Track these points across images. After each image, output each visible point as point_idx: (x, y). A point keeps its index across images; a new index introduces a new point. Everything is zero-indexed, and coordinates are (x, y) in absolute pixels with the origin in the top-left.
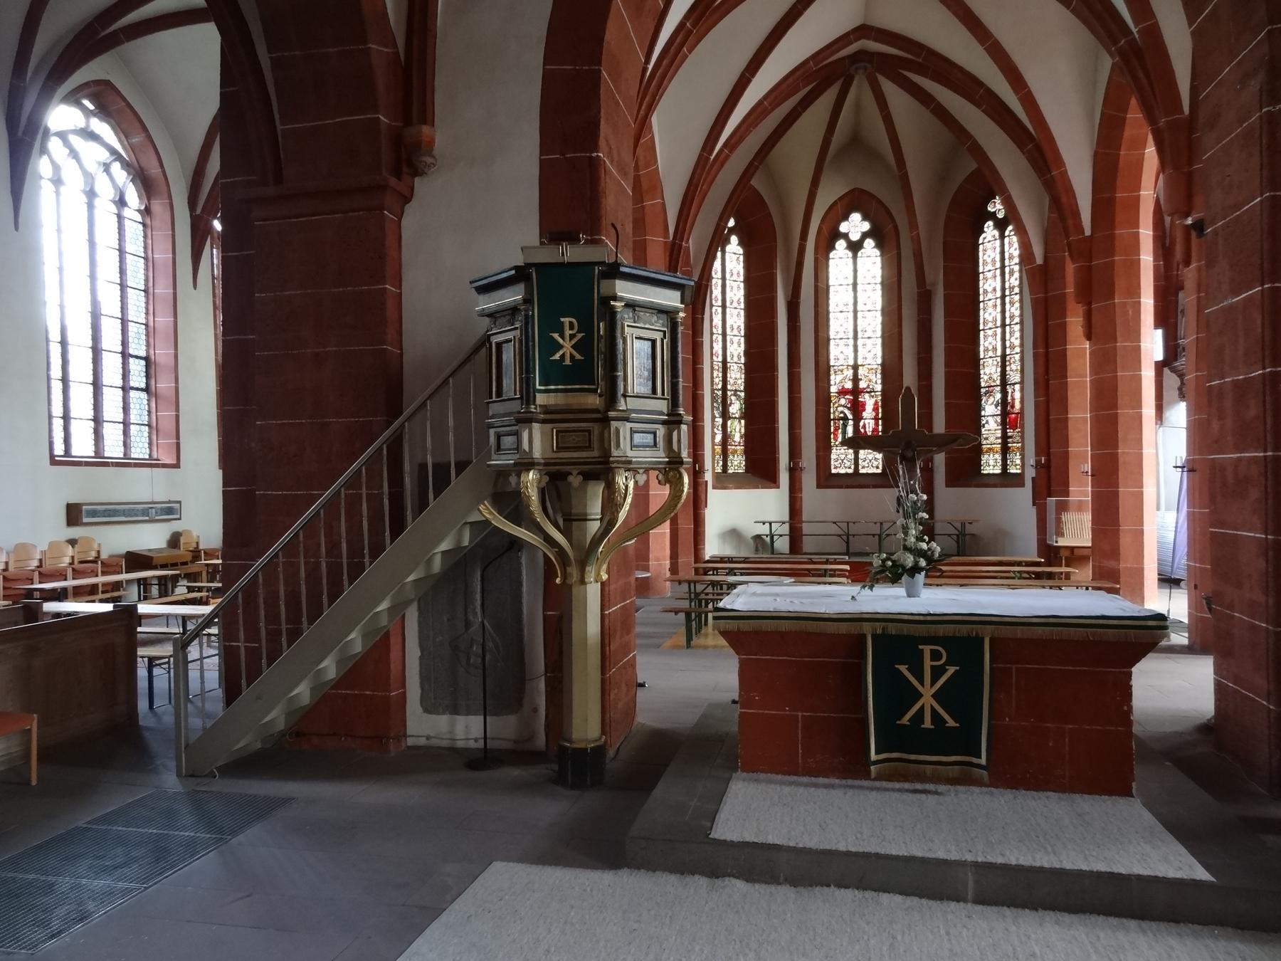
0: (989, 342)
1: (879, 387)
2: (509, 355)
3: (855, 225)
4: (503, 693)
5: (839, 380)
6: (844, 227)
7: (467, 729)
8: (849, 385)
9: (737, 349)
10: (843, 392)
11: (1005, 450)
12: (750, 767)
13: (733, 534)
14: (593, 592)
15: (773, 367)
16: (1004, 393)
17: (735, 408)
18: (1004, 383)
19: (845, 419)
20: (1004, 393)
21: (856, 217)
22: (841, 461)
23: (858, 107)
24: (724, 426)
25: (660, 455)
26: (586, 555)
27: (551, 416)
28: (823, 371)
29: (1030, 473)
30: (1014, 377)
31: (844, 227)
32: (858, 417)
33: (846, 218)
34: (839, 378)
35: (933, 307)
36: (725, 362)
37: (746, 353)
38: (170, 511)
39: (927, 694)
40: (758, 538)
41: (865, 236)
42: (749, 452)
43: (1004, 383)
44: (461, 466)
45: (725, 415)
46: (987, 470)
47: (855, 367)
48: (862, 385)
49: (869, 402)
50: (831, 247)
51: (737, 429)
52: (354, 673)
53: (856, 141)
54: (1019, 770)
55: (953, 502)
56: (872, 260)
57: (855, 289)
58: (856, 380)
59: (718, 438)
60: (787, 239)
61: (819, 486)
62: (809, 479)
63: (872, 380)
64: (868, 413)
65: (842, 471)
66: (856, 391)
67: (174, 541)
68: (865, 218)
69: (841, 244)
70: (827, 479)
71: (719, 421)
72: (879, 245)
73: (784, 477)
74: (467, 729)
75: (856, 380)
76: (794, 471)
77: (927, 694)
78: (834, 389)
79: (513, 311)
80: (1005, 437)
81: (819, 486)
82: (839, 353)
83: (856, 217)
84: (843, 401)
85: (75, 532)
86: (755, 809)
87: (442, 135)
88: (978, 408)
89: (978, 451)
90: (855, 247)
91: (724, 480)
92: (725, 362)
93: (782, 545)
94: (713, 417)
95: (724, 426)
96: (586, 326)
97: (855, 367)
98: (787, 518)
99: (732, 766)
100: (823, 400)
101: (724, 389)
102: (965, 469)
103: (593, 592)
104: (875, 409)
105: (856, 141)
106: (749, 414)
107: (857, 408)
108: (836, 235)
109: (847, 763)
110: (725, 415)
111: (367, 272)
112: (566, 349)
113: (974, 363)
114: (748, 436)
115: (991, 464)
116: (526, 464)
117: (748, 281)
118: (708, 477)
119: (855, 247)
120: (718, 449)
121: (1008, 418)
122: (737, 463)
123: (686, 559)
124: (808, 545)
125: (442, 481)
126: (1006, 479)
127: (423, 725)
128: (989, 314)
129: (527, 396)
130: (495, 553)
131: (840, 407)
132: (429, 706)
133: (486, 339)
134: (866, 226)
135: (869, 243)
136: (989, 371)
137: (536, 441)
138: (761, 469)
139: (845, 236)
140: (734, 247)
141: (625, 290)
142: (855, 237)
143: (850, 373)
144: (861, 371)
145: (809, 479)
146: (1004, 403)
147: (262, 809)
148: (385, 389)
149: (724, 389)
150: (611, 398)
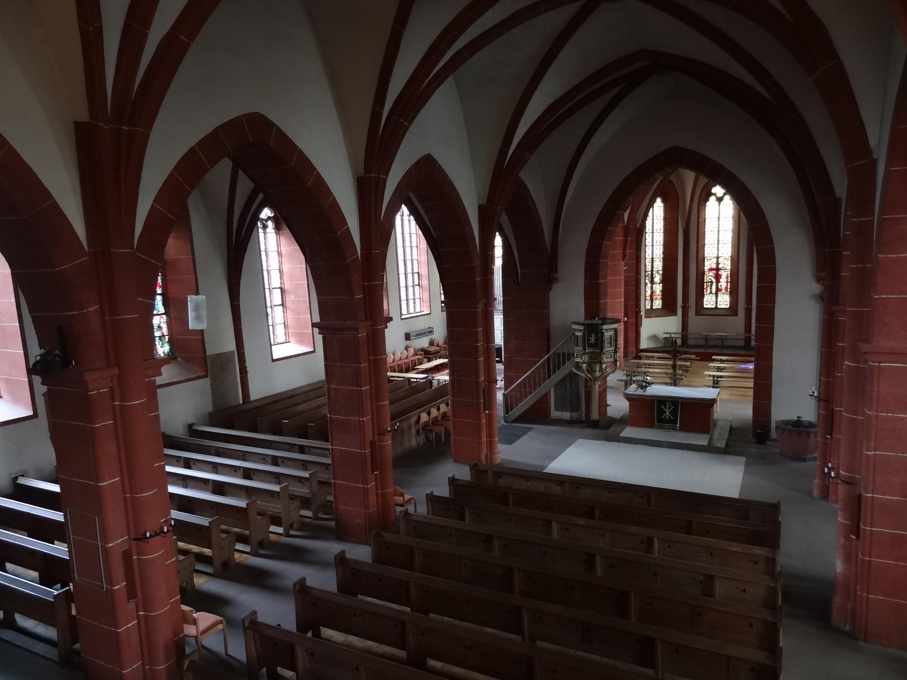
1: (729, 267)
4: (575, 408)
5: (709, 264)
6: (714, 190)
7: (566, 415)
8: (714, 266)
9: (659, 252)
10: (711, 270)
12: (632, 425)
13: (654, 337)
14: (597, 387)
17: (657, 279)
19: (712, 282)
22: (709, 302)
24: (652, 288)
25: (612, 360)
26: (596, 379)
27: (589, 353)
28: (701, 260)
32: (718, 281)
34: (710, 262)
36: (652, 259)
37: (664, 253)
38: (431, 332)
40: (666, 338)
42: (664, 298)
45: (652, 282)
47: (718, 258)
48: (720, 266)
49: (724, 275)
50: (707, 200)
51: (658, 288)
52: (539, 402)
54: (686, 428)
56: (728, 205)
58: (718, 264)
59: (649, 293)
61: (697, 314)
62: (692, 312)
63: (726, 264)
64: (723, 280)
65: (709, 306)
66: (718, 269)
67: (432, 343)
69: (712, 198)
71: (649, 285)
73: (680, 311)
74: (566, 415)
75: (718, 264)
76: (685, 309)
78: (706, 268)
82: (710, 251)
84: (711, 274)
85: (408, 343)
86: (629, 432)
91: (651, 313)
92: (652, 259)
93: (679, 342)
94: (646, 284)
95: (652, 288)
96: (597, 335)
99: (627, 425)
100: (701, 274)
101: (652, 271)
103: (597, 387)
104: (727, 278)
106: (663, 281)
107: (718, 277)
109: (651, 425)
110: (652, 282)
111: (542, 307)
112: (592, 341)
114: (663, 292)
117: (666, 219)
118: (643, 313)
119: (720, 200)
120: (648, 298)
122: (658, 304)
123: (632, 349)
124: (691, 342)
127: (555, 414)
129: (584, 349)
130: (572, 376)
131: (709, 276)
132: (557, 409)
138: (669, 308)
139: (715, 194)
140: (659, 200)
141: (605, 327)
142: (720, 194)
143: (715, 260)
144: (720, 260)
147: (531, 429)
148: (546, 336)
149: (652, 271)
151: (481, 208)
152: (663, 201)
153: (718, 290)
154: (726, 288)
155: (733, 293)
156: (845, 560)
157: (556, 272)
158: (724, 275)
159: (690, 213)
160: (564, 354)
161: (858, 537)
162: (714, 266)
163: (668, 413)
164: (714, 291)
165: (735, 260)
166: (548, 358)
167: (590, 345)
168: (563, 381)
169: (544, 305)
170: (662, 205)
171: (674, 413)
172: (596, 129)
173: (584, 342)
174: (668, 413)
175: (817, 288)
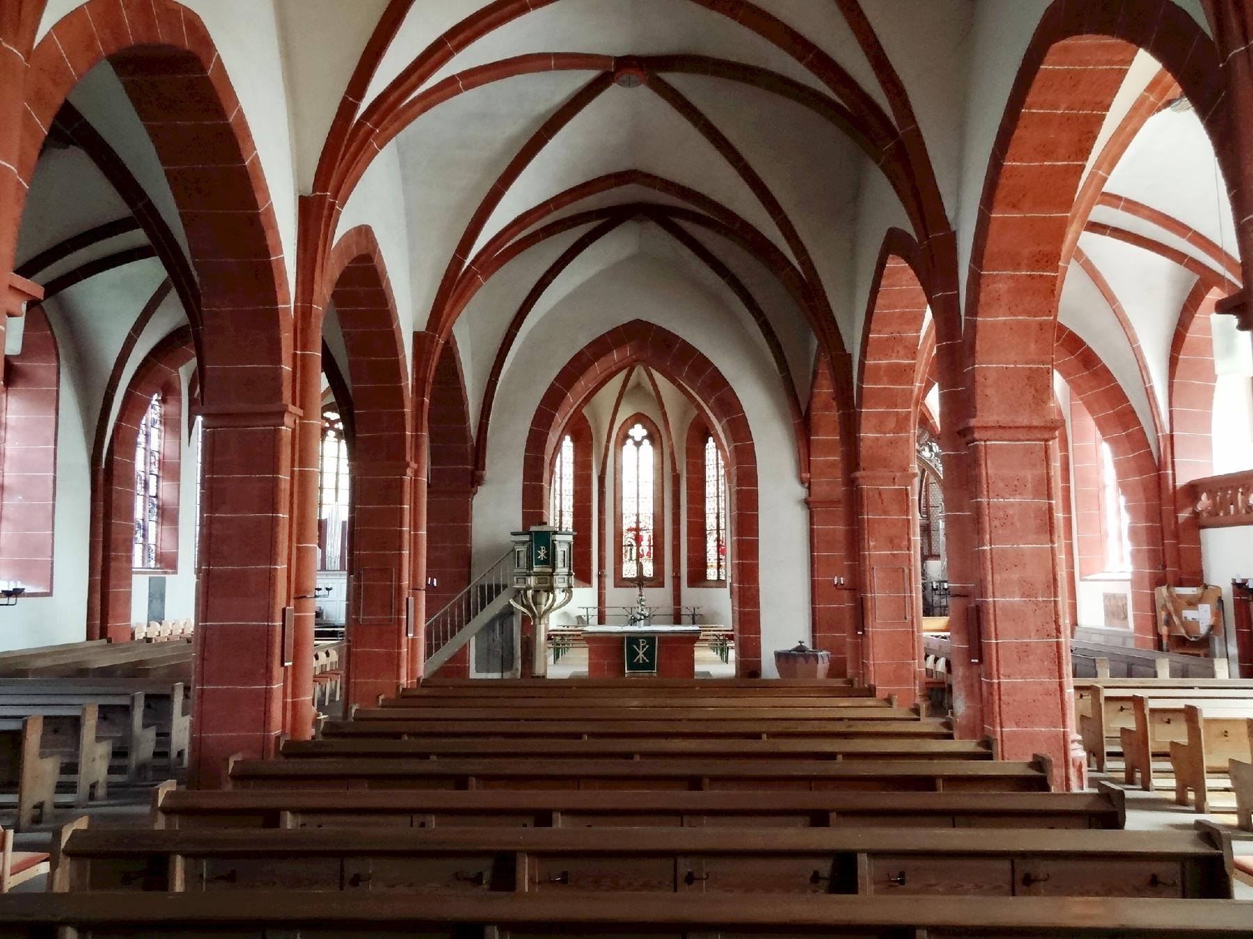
0: (710, 506)
1: (651, 527)
2: (522, 555)
3: (638, 431)
4: (506, 664)
5: (628, 522)
6: (631, 432)
8: (634, 526)
10: (630, 530)
11: (719, 566)
15: (589, 515)
16: (718, 533)
18: (718, 529)
19: (631, 545)
20: (718, 533)
21: (638, 427)
22: (629, 570)
23: (639, 374)
25: (565, 585)
27: (537, 574)
28: (618, 518)
29: (729, 581)
30: (722, 526)
31: (631, 432)
32: (639, 545)
33: (632, 427)
35: (680, 485)
36: (561, 511)
37: (574, 506)
39: (641, 653)
40: (579, 617)
41: (644, 438)
43: (718, 529)
44: (505, 587)
46: (709, 577)
47: (638, 515)
48: (641, 526)
50: (623, 443)
53: (638, 386)
55: (691, 596)
57: (637, 470)
58: (638, 522)
60: (599, 442)
61: (616, 586)
62: (609, 581)
63: (647, 523)
66: (637, 530)
68: (644, 427)
69: (629, 442)
70: (621, 582)
72: (653, 443)
75: (638, 522)
76: (600, 577)
77: (641, 653)
78: (625, 528)
79: (524, 543)
80: (719, 559)
81: (616, 586)
82: (628, 508)
83: (638, 427)
87: (488, 473)
88: (705, 542)
89: (705, 566)
90: (638, 444)
92: (561, 511)
96: (547, 549)
97: (638, 515)
98: (596, 605)
100: (619, 535)
102: (698, 577)
105: (638, 386)
107: (638, 539)
108: (627, 437)
112: (542, 555)
113: (703, 515)
115: (712, 574)
116: (529, 588)
117: (575, 462)
119: (638, 444)
121: (720, 549)
125: (498, 592)
126: (720, 583)
128: (710, 489)
129: (530, 567)
131: (628, 538)
133: (513, 550)
134: (645, 432)
135: (646, 442)
136: (711, 522)
137: (532, 581)
139: (633, 438)
140: (568, 438)
142: (638, 439)
145: (609, 581)
146: (718, 540)
150: (554, 570)
151: (417, 336)
152: (573, 440)
153: (639, 556)
154: (649, 554)
155: (658, 560)
156: (967, 696)
157: (483, 469)
158: (647, 536)
159: (606, 456)
160: (490, 587)
161: (981, 660)
162: (634, 526)
163: (641, 655)
164: (634, 557)
165: (658, 520)
166: (469, 592)
167: (539, 562)
168: (490, 626)
169: (464, 515)
170: (571, 444)
171: (649, 654)
172: (695, 124)
173: (529, 559)
174: (641, 655)
175: (801, 492)
